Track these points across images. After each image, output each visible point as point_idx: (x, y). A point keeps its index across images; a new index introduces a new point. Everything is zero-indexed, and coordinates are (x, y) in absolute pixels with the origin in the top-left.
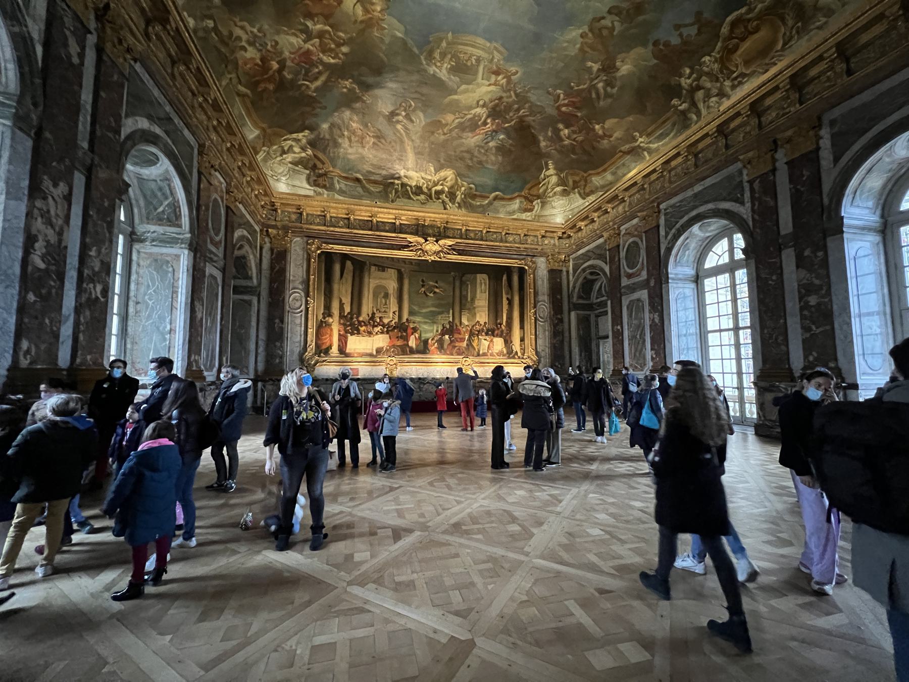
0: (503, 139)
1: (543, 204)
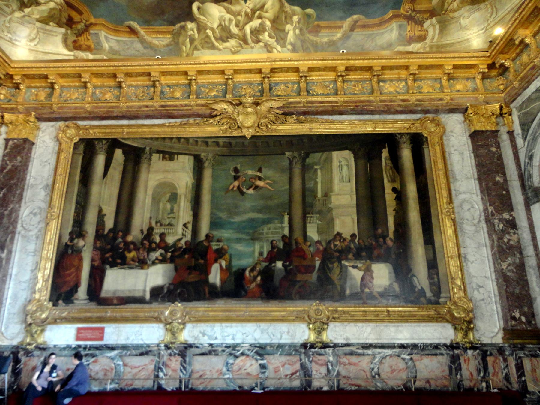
1: (444, 26)
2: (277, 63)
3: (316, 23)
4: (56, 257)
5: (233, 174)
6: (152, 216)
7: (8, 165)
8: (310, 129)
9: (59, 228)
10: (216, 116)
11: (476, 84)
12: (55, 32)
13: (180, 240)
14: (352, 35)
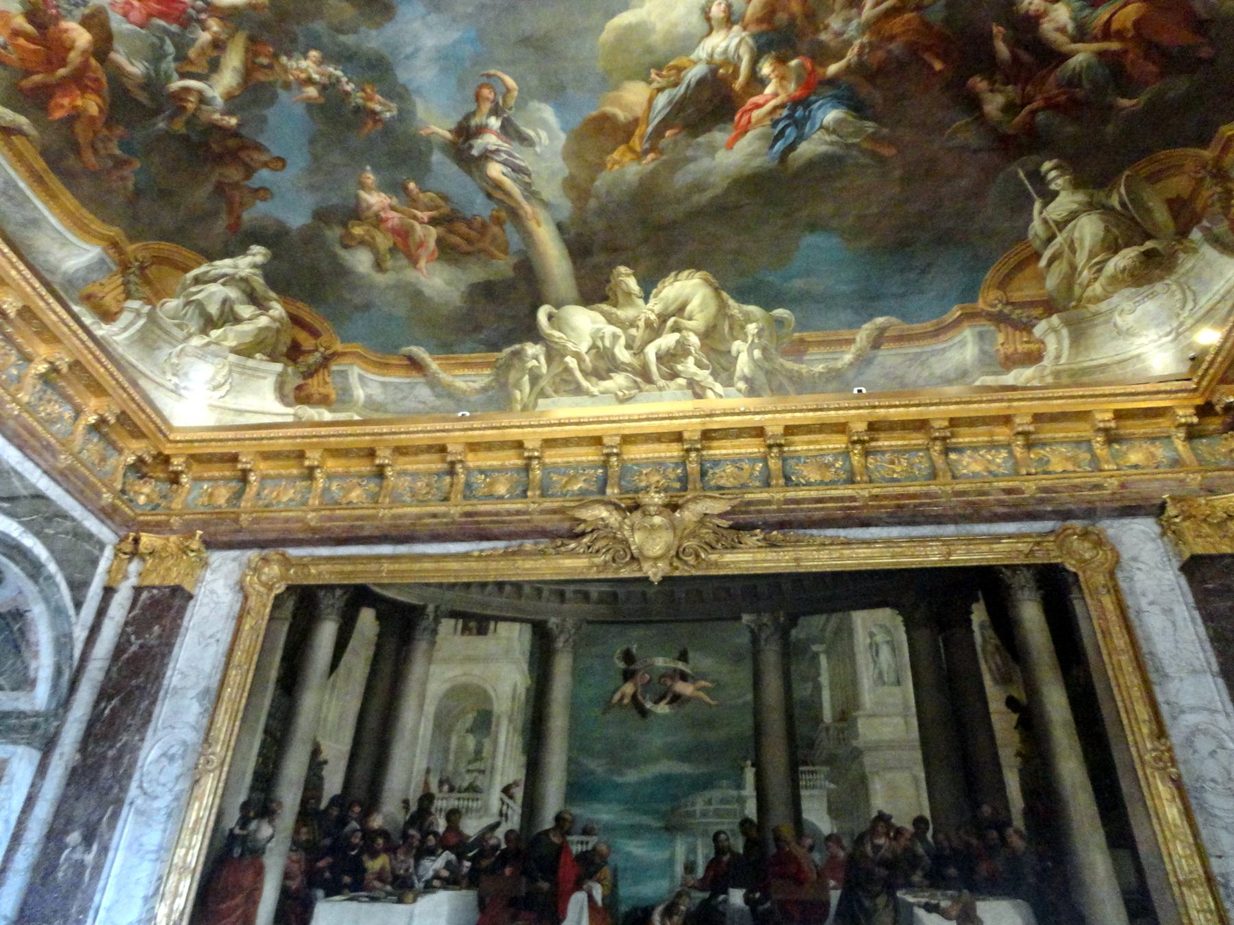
0: (839, 122)
1: (1079, 331)
2: (716, 419)
3: (796, 335)
4: (205, 864)
5: (621, 665)
6: (432, 766)
7: (131, 644)
8: (796, 560)
9: (220, 792)
10: (583, 534)
11: (1176, 450)
12: (263, 371)
13: (493, 827)
14: (875, 357)
